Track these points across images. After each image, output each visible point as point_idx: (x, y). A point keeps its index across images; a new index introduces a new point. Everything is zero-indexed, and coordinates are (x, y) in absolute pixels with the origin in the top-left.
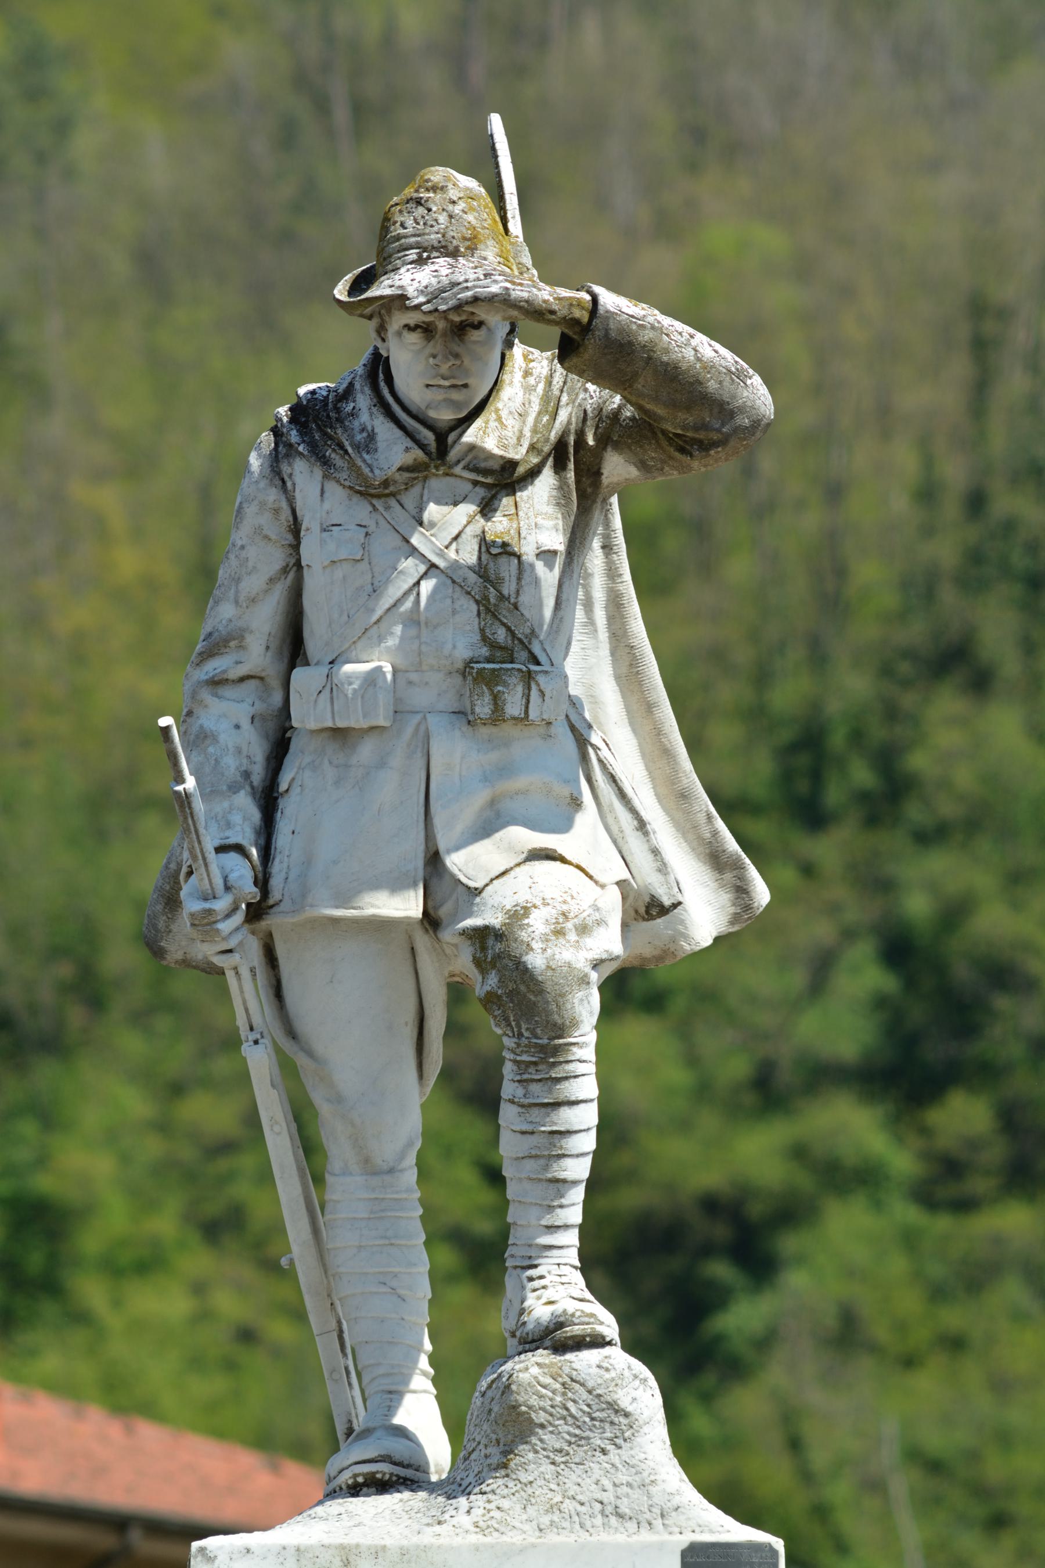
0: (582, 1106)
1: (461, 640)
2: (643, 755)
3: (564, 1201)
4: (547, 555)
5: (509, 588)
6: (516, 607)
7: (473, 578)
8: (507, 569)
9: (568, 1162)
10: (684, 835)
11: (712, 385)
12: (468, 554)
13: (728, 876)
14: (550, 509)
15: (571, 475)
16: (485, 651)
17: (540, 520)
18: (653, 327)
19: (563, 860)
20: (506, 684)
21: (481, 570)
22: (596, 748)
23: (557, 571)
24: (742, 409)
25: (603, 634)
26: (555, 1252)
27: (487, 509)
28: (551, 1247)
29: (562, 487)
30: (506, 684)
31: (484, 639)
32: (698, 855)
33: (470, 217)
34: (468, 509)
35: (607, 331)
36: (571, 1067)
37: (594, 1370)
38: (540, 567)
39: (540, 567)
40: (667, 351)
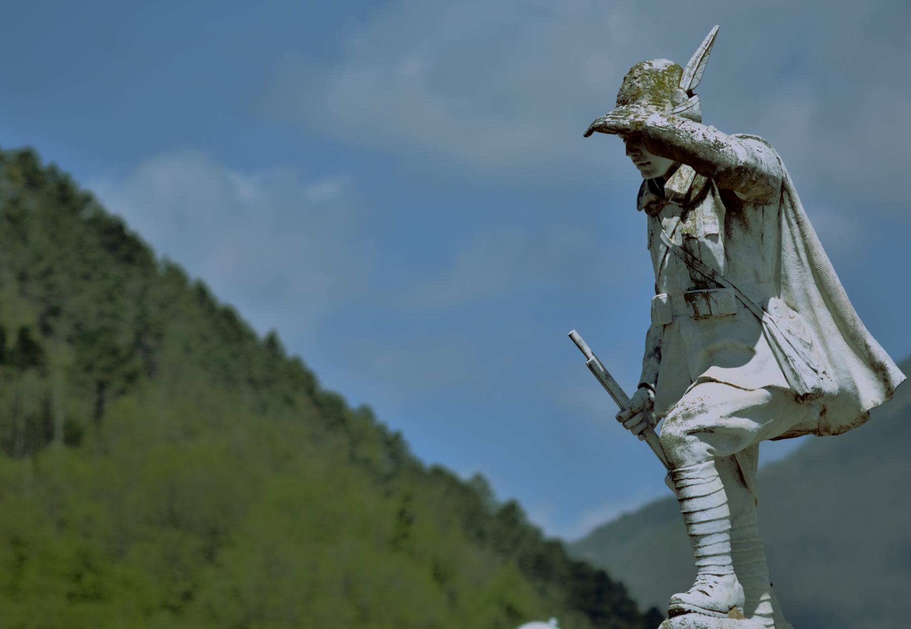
0: (694, 500)
1: (684, 282)
2: (835, 321)
3: (700, 545)
4: (712, 237)
5: (696, 254)
6: (701, 262)
7: (681, 251)
8: (693, 245)
9: (695, 526)
10: (859, 356)
11: (701, 155)
12: (677, 241)
13: (880, 373)
14: (713, 214)
15: (719, 197)
16: (693, 285)
17: (706, 220)
18: (670, 131)
19: (717, 382)
20: (696, 300)
21: (684, 248)
22: (766, 323)
23: (721, 243)
24: (718, 164)
25: (806, 265)
26: (702, 569)
27: (683, 218)
28: (700, 567)
29: (716, 203)
30: (696, 300)
31: (692, 279)
32: (867, 366)
33: (640, 85)
34: (676, 219)
35: (649, 135)
36: (683, 482)
37: (678, 625)
38: (709, 243)
39: (709, 243)
40: (678, 141)
